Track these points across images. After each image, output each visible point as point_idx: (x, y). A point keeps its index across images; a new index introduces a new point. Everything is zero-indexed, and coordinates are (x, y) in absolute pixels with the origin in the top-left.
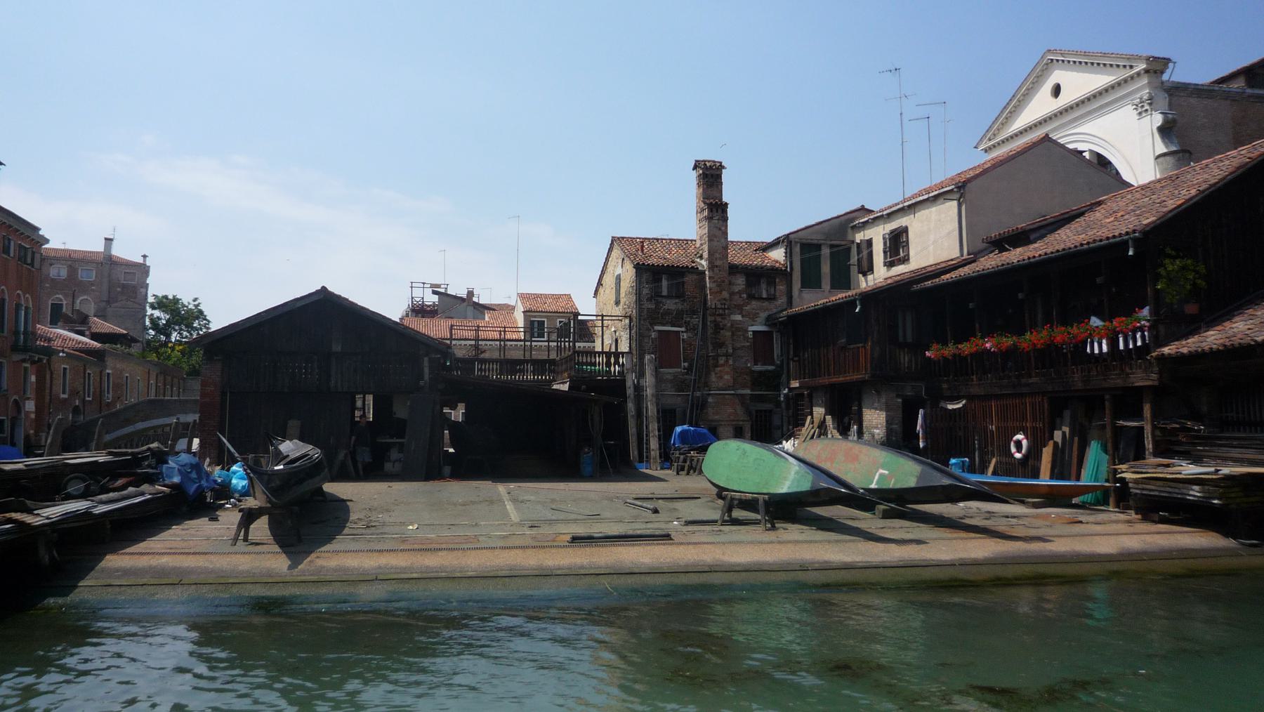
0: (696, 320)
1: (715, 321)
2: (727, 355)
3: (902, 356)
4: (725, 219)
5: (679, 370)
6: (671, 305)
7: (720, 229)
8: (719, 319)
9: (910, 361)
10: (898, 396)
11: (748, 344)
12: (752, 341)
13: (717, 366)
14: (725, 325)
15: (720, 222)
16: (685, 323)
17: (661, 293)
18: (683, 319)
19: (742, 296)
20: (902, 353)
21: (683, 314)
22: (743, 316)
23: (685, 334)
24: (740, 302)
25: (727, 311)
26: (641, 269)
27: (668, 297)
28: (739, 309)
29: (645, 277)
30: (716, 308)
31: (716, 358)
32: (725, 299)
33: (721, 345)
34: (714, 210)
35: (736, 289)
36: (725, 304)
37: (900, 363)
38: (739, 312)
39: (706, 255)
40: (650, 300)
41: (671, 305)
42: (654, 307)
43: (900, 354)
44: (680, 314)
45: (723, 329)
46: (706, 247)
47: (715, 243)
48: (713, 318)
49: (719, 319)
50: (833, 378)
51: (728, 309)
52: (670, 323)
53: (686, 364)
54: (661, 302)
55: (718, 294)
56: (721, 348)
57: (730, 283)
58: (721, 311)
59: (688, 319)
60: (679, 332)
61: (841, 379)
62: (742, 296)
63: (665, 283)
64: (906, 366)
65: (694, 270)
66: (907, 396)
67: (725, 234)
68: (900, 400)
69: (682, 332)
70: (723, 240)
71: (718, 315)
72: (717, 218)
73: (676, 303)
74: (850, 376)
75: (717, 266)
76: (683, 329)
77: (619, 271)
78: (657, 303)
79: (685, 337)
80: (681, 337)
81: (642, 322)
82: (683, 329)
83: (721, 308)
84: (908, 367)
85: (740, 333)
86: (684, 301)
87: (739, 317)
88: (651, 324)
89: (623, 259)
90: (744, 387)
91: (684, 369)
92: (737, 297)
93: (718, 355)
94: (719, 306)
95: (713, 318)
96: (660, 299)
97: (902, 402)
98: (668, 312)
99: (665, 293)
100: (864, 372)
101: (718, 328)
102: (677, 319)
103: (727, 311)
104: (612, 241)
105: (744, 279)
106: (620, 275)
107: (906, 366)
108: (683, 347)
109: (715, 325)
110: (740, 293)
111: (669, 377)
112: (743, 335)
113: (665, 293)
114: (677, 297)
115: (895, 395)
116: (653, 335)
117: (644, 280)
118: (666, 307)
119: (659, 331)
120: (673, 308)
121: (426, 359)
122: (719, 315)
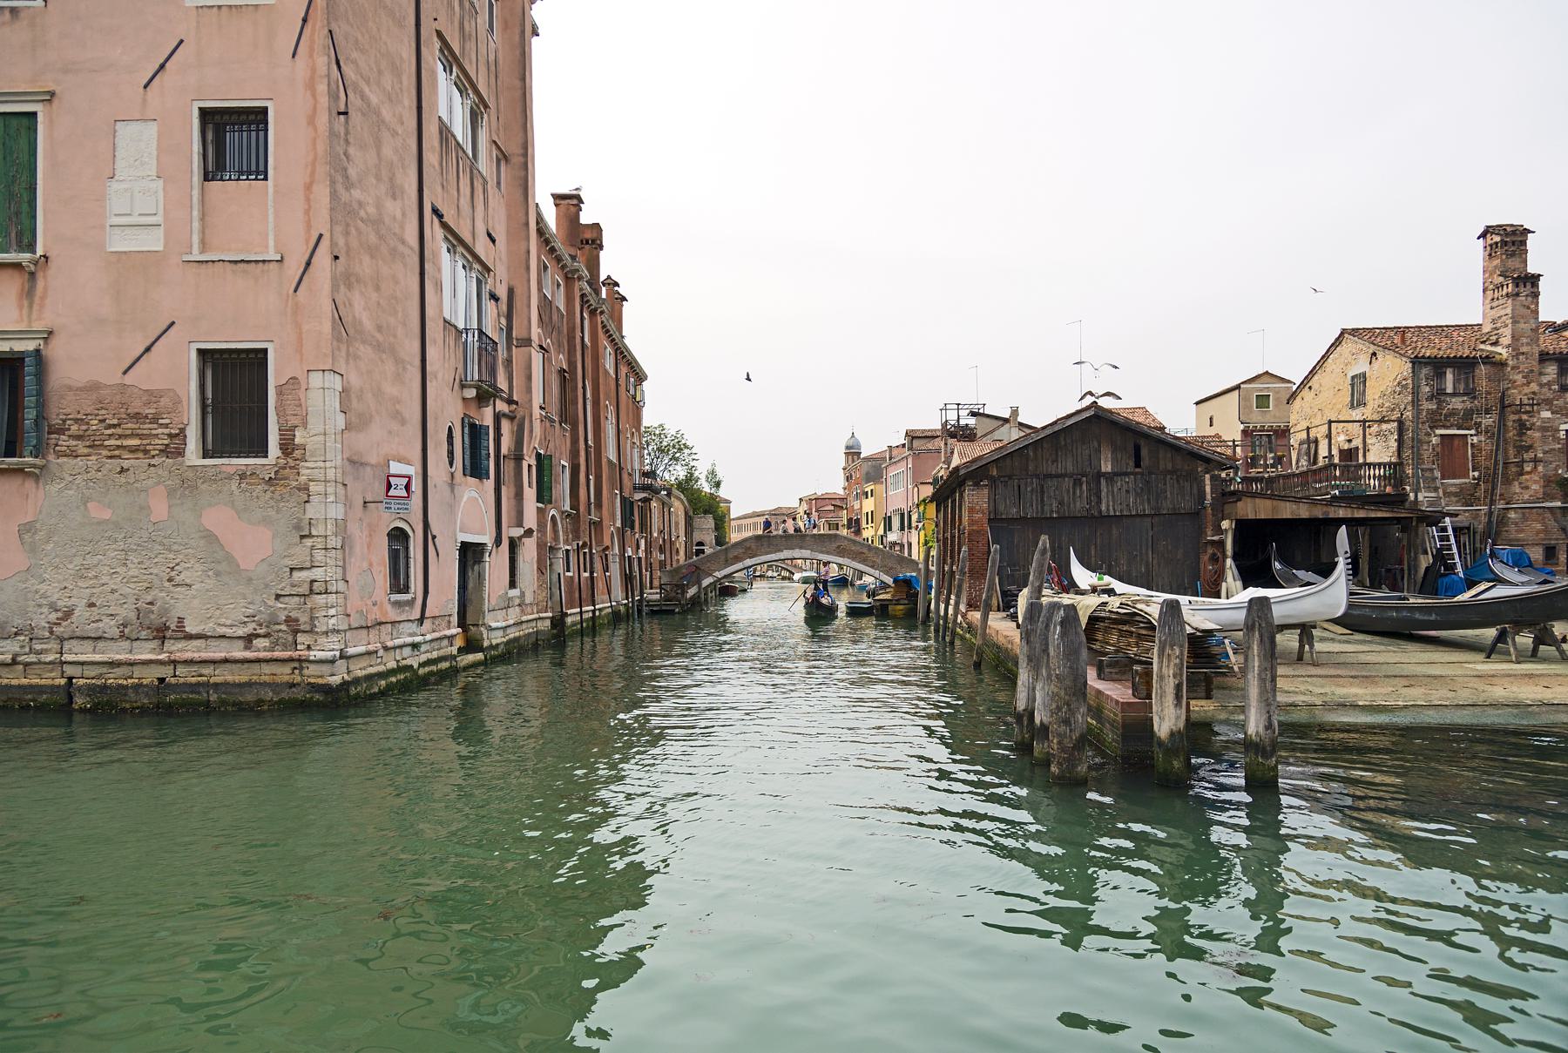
0: (1488, 421)
1: (1520, 420)
2: (1536, 461)
4: (1536, 295)
5: (1467, 481)
6: (1457, 404)
7: (1528, 308)
8: (1525, 417)
11: (1560, 446)
12: (1564, 442)
13: (1522, 475)
14: (1533, 424)
15: (1530, 299)
16: (1476, 423)
17: (1445, 389)
18: (1472, 419)
19: (1553, 387)
21: (1472, 415)
22: (1552, 413)
23: (1475, 438)
24: (1550, 395)
25: (1535, 407)
26: (1420, 363)
27: (1454, 394)
28: (1548, 403)
29: (1425, 371)
30: (1521, 405)
31: (1520, 464)
32: (1534, 393)
33: (1530, 447)
34: (1522, 285)
35: (1545, 380)
36: (1533, 399)
38: (1547, 407)
39: (1506, 340)
40: (1430, 399)
41: (1457, 404)
42: (1435, 407)
44: (1468, 414)
45: (1530, 429)
46: (1507, 332)
47: (1522, 325)
48: (1516, 417)
49: (1525, 417)
51: (1538, 404)
52: (1456, 425)
53: (1476, 474)
54: (1444, 401)
55: (1525, 388)
56: (1527, 452)
57: (1541, 374)
58: (1528, 408)
59: (1479, 420)
60: (1466, 435)
62: (1553, 387)
63: (1449, 376)
65: (1488, 360)
67: (1536, 312)
69: (1471, 435)
70: (1532, 321)
71: (1524, 413)
72: (1525, 294)
73: (1463, 402)
75: (1523, 353)
76: (1473, 432)
77: (1361, 366)
78: (1439, 403)
79: (1475, 441)
80: (1470, 441)
81: (1420, 426)
82: (1473, 432)
83: (1529, 405)
85: (1549, 433)
86: (1474, 398)
87: (1546, 414)
88: (1431, 428)
89: (1374, 354)
90: (1553, 499)
91: (1474, 479)
92: (1545, 390)
93: (1523, 461)
94: (1526, 402)
95: (1516, 417)
96: (1443, 398)
98: (1453, 413)
99: (1449, 390)
101: (1522, 427)
102: (1466, 419)
103: (1535, 407)
104: (1342, 334)
105: (1555, 367)
106: (1364, 375)
108: (1473, 453)
109: (1520, 425)
110: (1549, 384)
111: (1453, 489)
112: (1553, 436)
113: (1449, 390)
114: (1465, 394)
116: (1435, 440)
117: (1422, 376)
118: (1450, 407)
119: (1442, 436)
120: (1460, 407)
121: (1207, 476)
122: (1526, 412)
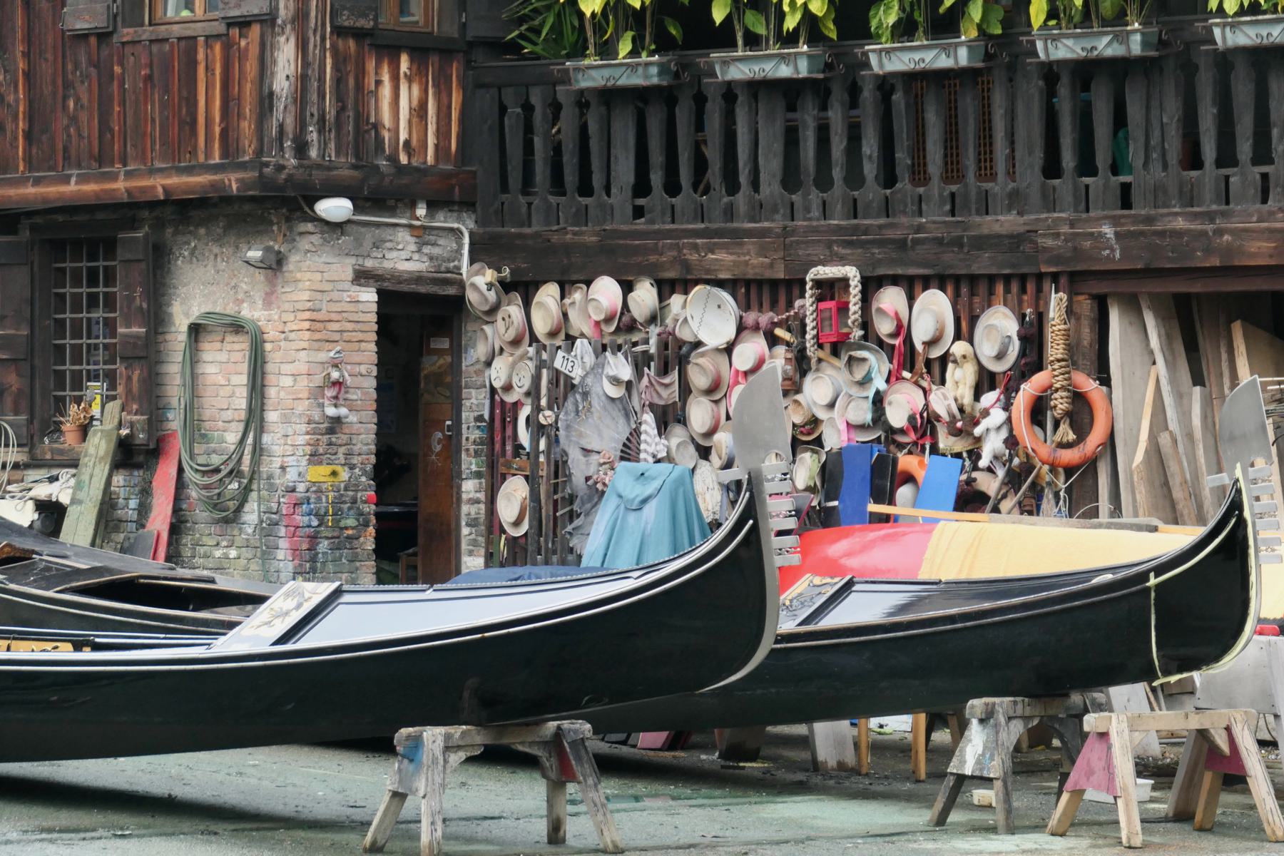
3: (386, 91)
9: (420, 112)
10: (362, 277)
20: (386, 78)
37: (377, 126)
43: (379, 83)
50: (22, 181)
61: (72, 188)
64: (403, 136)
66: (396, 277)
68: (369, 296)
74: (129, 175)
84: (407, 143)
97: (379, 303)
100: (216, 159)
107: (403, 136)
115: (344, 269)
